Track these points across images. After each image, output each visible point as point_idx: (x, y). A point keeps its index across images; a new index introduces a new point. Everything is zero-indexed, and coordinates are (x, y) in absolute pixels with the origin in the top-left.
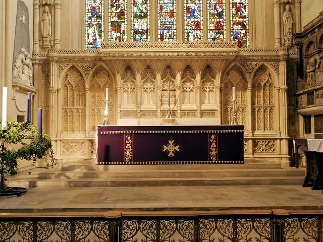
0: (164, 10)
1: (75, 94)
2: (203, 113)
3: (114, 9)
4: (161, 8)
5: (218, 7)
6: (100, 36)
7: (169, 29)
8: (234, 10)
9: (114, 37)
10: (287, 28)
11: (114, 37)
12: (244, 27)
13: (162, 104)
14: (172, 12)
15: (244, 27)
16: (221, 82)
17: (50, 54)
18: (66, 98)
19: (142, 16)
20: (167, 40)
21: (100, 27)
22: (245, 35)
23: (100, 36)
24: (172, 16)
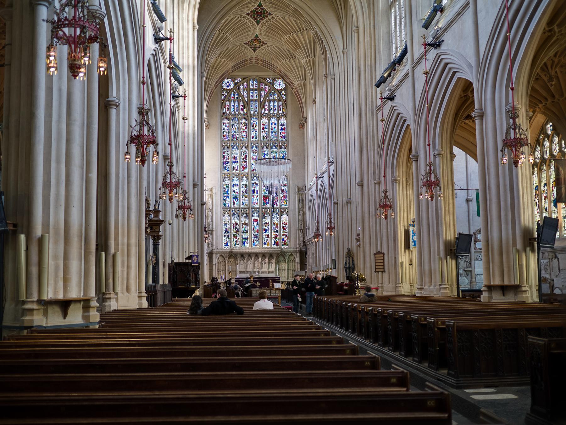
0: (255, 230)
1: (222, 265)
2: (269, 272)
3: (234, 229)
4: (253, 229)
5: (276, 228)
6: (229, 240)
7: (256, 237)
8: (282, 229)
9: (235, 241)
10: (301, 239)
11: (235, 241)
12: (287, 236)
13: (254, 269)
14: (258, 230)
15: (287, 236)
16: (276, 261)
17: (213, 251)
18: (218, 267)
19: (245, 232)
20: (256, 242)
21: (229, 237)
22: (287, 239)
23: (229, 240)
24: (258, 232)
